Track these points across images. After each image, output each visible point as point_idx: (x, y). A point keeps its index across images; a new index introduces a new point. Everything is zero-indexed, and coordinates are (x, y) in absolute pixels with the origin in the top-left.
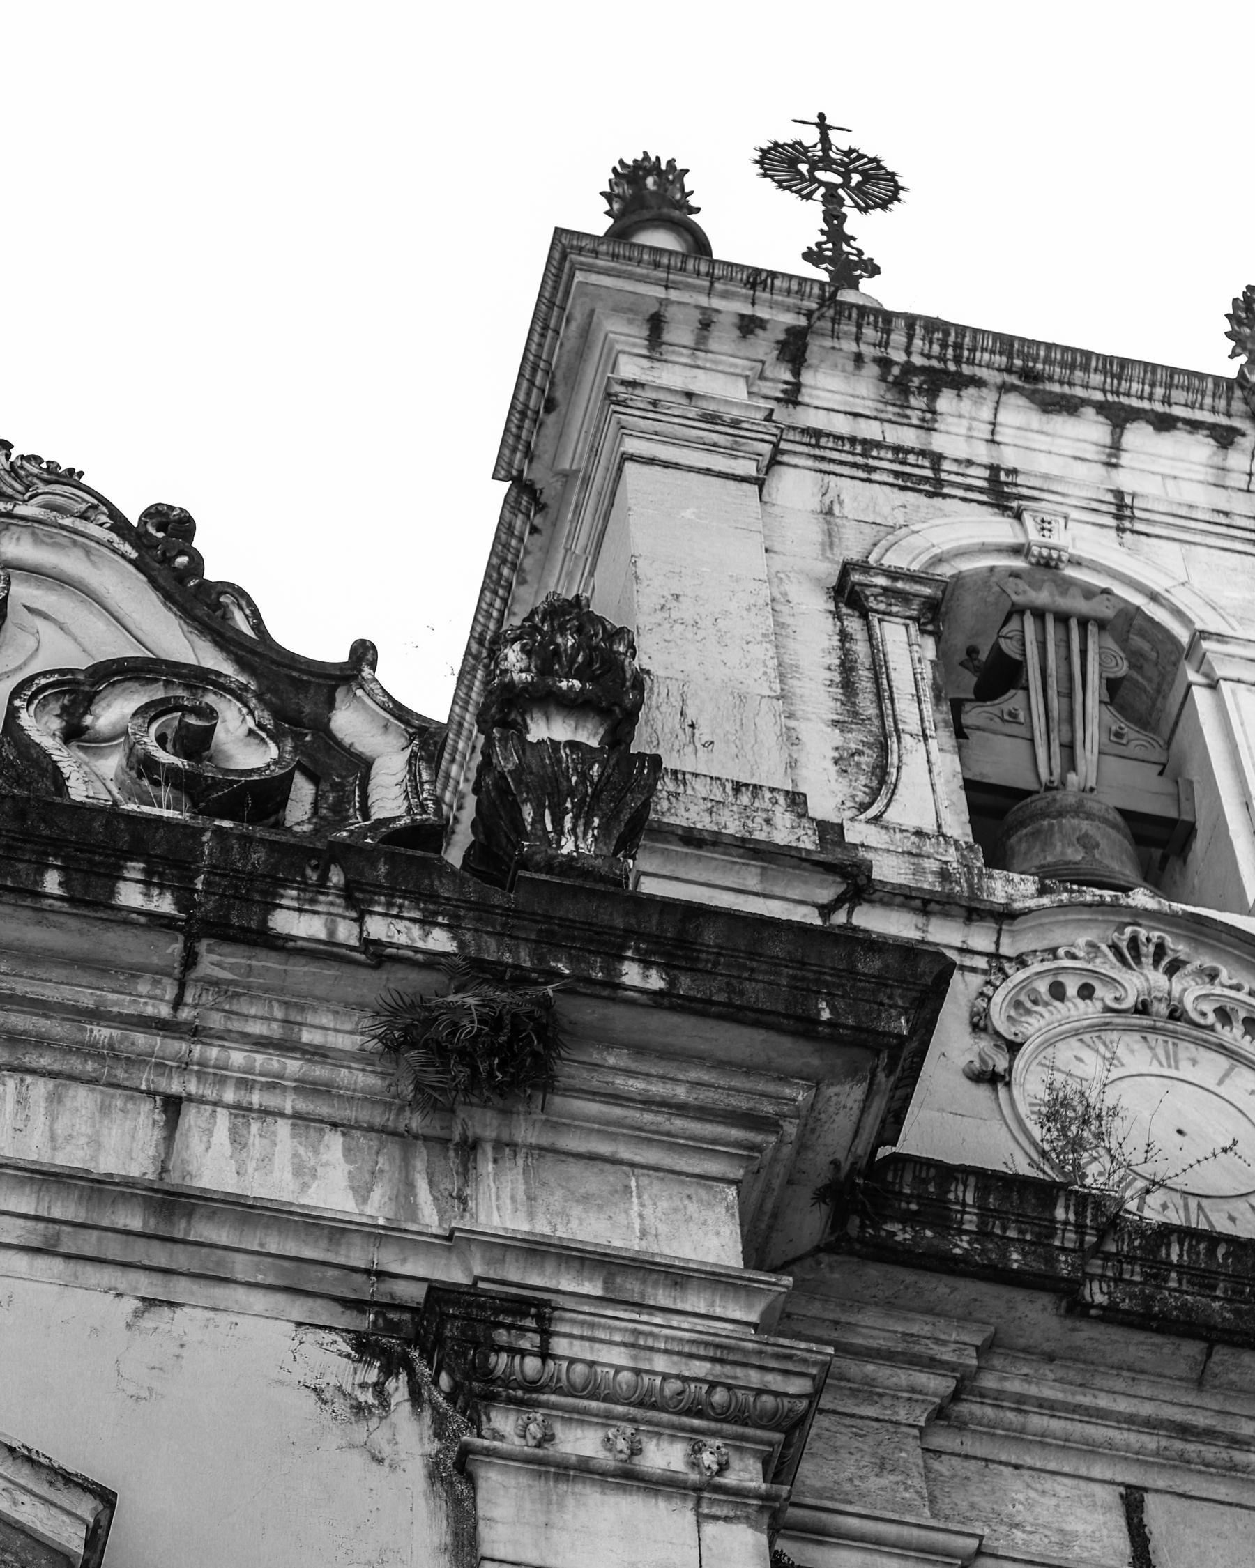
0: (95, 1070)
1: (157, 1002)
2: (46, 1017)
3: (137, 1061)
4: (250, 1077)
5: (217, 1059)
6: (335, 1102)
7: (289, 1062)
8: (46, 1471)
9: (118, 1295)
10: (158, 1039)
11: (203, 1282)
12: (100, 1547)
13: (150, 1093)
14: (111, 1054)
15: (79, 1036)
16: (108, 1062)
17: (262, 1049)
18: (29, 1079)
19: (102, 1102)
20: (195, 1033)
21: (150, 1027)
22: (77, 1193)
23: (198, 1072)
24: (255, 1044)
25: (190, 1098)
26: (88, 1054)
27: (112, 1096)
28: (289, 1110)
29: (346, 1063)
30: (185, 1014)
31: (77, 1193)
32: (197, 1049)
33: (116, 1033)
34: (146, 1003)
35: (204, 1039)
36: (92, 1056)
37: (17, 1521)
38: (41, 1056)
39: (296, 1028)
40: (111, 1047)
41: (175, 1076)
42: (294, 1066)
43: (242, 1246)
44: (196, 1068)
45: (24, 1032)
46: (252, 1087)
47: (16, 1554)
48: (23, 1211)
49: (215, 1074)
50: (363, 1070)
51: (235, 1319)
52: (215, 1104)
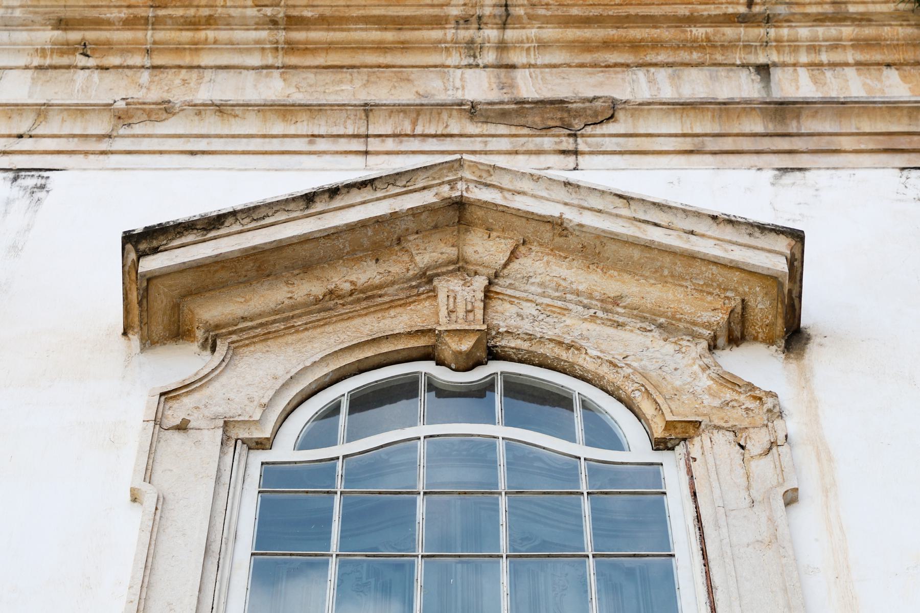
0: (699, 58)
1: (735, 6)
2: (655, 27)
3: (729, 46)
4: (817, 43)
5: (788, 35)
6: (885, 51)
7: (844, 29)
8: (744, 227)
9: (759, 169)
10: (742, 29)
11: (820, 155)
12: (798, 278)
13: (743, 66)
14: (709, 44)
15: (683, 36)
16: (708, 51)
17: (821, 24)
18: (652, 70)
19: (710, 75)
20: (768, 20)
21: (734, 22)
22: (710, 114)
23: (776, 47)
24: (815, 21)
25: (775, 65)
26: (692, 47)
27: (717, 71)
28: (851, 61)
29: (886, 23)
30: (757, 9)
31: (710, 114)
32: (772, 32)
33: (710, 30)
34: (727, 8)
35: (775, 24)
36: (695, 48)
37: (731, 261)
38: (658, 54)
39: (843, 6)
40: (708, 40)
41: (760, 51)
42: (848, 31)
43: (844, 131)
44: (774, 44)
45: (642, 40)
46: (819, 51)
47: (735, 290)
48: (673, 131)
49: (789, 46)
50: (901, 25)
51: (852, 172)
52: (795, 65)
